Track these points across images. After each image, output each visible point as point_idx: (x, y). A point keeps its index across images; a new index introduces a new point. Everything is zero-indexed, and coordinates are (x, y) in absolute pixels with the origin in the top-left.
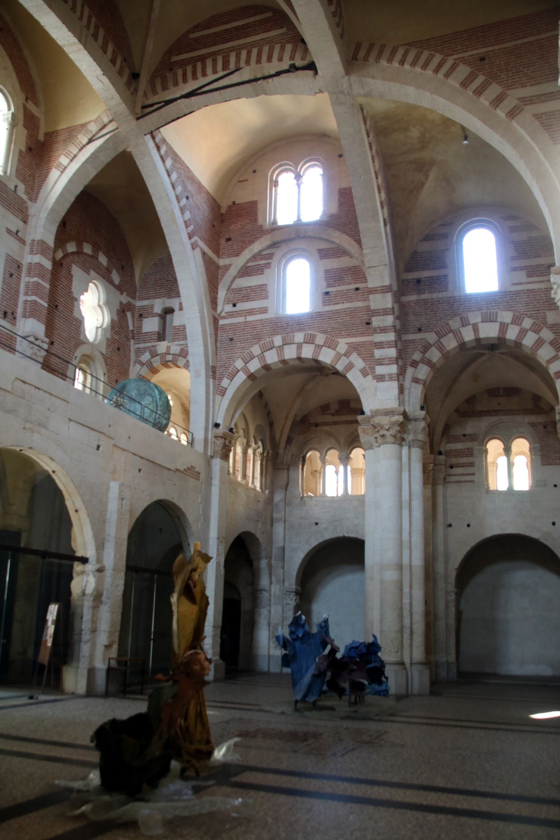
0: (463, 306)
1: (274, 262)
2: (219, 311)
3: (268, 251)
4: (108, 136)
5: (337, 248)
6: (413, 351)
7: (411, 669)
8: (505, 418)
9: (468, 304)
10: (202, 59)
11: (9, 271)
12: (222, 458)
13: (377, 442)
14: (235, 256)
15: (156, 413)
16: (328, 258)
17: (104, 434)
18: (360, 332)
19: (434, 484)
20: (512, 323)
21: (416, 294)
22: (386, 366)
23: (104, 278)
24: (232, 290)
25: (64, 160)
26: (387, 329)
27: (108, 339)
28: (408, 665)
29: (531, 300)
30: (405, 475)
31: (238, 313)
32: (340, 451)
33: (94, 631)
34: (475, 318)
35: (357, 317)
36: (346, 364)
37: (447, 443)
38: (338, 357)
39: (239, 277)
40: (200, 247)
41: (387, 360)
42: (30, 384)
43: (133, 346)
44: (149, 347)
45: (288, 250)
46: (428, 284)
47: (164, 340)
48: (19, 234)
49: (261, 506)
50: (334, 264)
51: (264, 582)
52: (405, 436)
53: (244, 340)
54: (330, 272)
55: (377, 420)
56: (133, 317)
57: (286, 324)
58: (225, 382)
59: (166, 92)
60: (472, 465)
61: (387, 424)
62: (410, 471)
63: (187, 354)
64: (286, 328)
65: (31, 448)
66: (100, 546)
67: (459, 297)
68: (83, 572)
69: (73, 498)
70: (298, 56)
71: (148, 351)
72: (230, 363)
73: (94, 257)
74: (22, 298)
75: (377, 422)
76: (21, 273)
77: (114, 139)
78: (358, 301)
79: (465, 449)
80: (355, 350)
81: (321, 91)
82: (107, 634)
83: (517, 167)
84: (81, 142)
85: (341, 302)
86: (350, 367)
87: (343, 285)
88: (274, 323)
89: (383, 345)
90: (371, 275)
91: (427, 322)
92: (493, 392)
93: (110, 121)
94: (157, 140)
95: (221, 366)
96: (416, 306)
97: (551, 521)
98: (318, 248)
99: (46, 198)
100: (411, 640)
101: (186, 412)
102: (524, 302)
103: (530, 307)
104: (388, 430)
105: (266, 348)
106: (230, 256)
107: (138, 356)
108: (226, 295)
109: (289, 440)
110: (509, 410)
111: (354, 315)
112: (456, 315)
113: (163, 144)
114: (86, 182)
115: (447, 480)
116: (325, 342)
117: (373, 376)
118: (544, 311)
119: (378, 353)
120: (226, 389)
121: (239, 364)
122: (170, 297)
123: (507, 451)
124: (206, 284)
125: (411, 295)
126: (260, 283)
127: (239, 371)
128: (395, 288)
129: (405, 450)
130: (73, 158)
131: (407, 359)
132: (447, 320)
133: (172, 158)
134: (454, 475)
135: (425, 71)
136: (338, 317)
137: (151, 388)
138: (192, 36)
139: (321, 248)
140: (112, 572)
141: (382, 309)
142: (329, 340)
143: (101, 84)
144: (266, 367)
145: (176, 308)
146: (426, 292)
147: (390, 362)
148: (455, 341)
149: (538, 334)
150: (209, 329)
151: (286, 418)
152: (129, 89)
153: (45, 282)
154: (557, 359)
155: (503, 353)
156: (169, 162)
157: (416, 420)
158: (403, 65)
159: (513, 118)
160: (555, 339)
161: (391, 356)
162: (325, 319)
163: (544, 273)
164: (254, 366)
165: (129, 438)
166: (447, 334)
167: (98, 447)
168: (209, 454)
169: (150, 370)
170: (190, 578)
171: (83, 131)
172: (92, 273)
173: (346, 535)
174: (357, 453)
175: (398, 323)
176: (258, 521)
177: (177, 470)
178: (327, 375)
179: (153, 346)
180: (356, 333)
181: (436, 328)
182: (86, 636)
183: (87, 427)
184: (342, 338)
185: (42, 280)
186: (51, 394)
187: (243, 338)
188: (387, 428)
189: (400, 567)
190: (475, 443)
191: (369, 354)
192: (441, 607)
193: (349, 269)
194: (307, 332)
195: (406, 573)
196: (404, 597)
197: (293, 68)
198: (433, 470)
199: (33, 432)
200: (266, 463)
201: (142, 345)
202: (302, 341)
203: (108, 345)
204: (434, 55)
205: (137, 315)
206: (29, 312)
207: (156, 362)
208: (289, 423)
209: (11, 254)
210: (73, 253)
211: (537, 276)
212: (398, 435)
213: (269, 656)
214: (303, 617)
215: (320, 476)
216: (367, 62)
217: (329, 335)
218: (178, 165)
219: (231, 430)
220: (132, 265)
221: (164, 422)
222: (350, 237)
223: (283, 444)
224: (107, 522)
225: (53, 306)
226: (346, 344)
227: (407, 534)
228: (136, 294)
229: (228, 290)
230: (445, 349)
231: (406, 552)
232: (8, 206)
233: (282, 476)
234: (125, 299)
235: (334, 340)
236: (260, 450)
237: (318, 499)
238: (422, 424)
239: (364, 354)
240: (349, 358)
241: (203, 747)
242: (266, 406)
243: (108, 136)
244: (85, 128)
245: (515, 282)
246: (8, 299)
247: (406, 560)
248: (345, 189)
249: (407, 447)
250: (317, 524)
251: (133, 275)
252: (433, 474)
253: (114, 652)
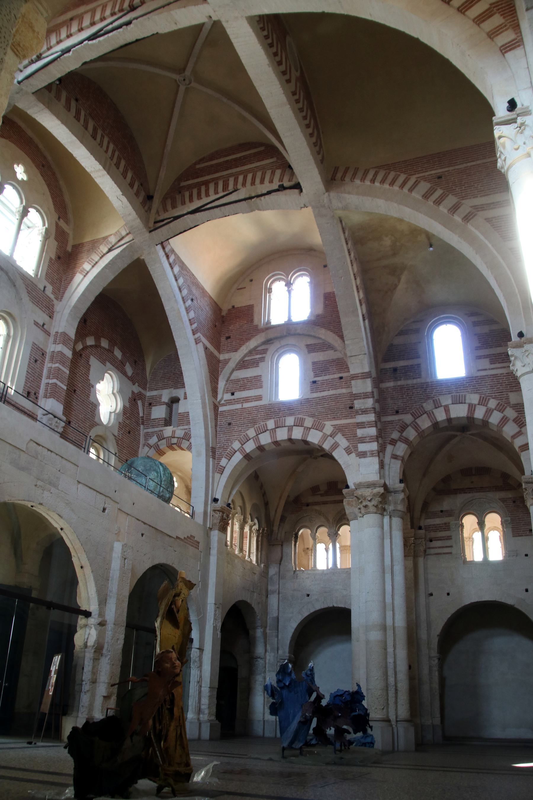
0: (435, 390)
1: (268, 356)
2: (218, 400)
3: (263, 347)
4: (125, 246)
5: (323, 343)
6: (392, 431)
7: (396, 726)
8: (477, 495)
9: (439, 388)
10: (206, 183)
11: (34, 357)
12: (219, 530)
13: (360, 512)
14: (234, 352)
15: (161, 486)
16: (315, 352)
17: (110, 498)
18: (344, 416)
19: (415, 557)
20: (479, 404)
21: (394, 381)
22: (367, 444)
23: (118, 369)
24: (230, 381)
25: (87, 266)
26: (367, 411)
27: (120, 423)
28: (393, 723)
29: (494, 384)
30: (387, 542)
31: (236, 400)
32: (329, 528)
33: (94, 682)
34: (446, 400)
35: (341, 403)
36: (332, 444)
37: (426, 519)
38: (325, 437)
39: (236, 370)
40: (203, 343)
41: (369, 438)
42: (43, 447)
43: (143, 431)
44: (157, 432)
45: (279, 346)
46: (403, 372)
47: (170, 425)
48: (45, 327)
49: (256, 577)
50: (320, 356)
51: (260, 650)
52: (386, 506)
53: (241, 425)
54: (317, 364)
55: (359, 492)
56: (143, 405)
57: (278, 409)
58: (223, 462)
59: (175, 210)
60: (449, 538)
61: (369, 496)
62: (391, 539)
63: (190, 437)
64: (278, 413)
65: (41, 504)
66: (103, 602)
67: (431, 382)
68: (86, 626)
69: (79, 555)
70: (286, 178)
71: (156, 435)
72: (228, 444)
73: (110, 351)
74: (44, 381)
75: (360, 493)
76: (45, 360)
77: (131, 248)
78: (342, 388)
79: (442, 524)
80: (339, 431)
81: (305, 206)
82: (106, 685)
83: (474, 262)
84: (102, 252)
85: (327, 389)
86: (336, 446)
87: (329, 375)
88: (267, 409)
89: (364, 425)
90: (352, 363)
91: (403, 405)
92: (466, 472)
93: (127, 234)
94: (167, 250)
95: (220, 447)
96: (393, 391)
97: (524, 588)
98: (306, 344)
99: (70, 297)
100: (396, 697)
101: (189, 491)
102: (489, 386)
103: (494, 390)
104: (370, 501)
105: (260, 431)
106: (229, 351)
107: (146, 439)
108: (226, 385)
109: (283, 519)
110: (481, 488)
111: (338, 401)
112: (428, 398)
113: (172, 254)
114: (104, 283)
115: (427, 553)
116: (313, 425)
117: (356, 454)
118: (507, 393)
119: (360, 432)
120: (225, 468)
121: (236, 445)
122: (176, 388)
123: (481, 525)
124: (208, 374)
125: (388, 382)
126: (255, 374)
127: (236, 452)
128: (374, 375)
129: (386, 519)
130: (95, 264)
131: (386, 438)
132: (421, 403)
133: (179, 266)
134: (433, 548)
135: (392, 187)
136: (324, 403)
137: (156, 465)
138: (198, 166)
139: (309, 343)
140: (113, 626)
141: (363, 393)
142: (316, 423)
143: (121, 202)
144: (261, 448)
145: (182, 397)
146: (402, 379)
147: (371, 440)
148: (429, 421)
149: (502, 413)
150: (210, 414)
151: (280, 498)
152: (144, 207)
153: (65, 368)
154: (521, 434)
155: (472, 435)
156: (176, 269)
157: (396, 492)
158: (374, 183)
159: (468, 222)
160: (518, 416)
161: (372, 435)
162: (313, 405)
163: (505, 360)
164: (250, 447)
165: (133, 504)
166: (422, 415)
167: (104, 510)
168: (208, 526)
169: (157, 452)
170: (173, 602)
171: (104, 242)
172: (108, 364)
173: (335, 605)
174: (344, 530)
175: (377, 406)
176: (254, 592)
177: (178, 538)
178: (316, 458)
179: (160, 431)
180: (341, 416)
181: (412, 410)
182: (86, 687)
183: (94, 490)
184: (328, 421)
185: (63, 366)
186: (62, 457)
187: (239, 423)
188: (369, 499)
189: (384, 628)
190: (451, 518)
191: (352, 434)
192: (425, 671)
193: (334, 361)
194: (297, 416)
195: (390, 633)
196: (388, 656)
197: (282, 188)
198: (414, 543)
199: (43, 490)
200: (262, 539)
201: (150, 430)
202: (293, 424)
203: (120, 428)
204: (399, 175)
205: (146, 404)
206: (49, 393)
207: (163, 445)
208: (283, 503)
209: (36, 343)
210: (91, 346)
211: (499, 363)
212: (380, 506)
213: (264, 721)
214: (290, 666)
215: (312, 553)
216: (344, 182)
217: (316, 418)
218: (185, 272)
219: (229, 505)
220: (144, 361)
221: (168, 496)
222: (334, 333)
223: (277, 523)
224: (110, 579)
225: (72, 390)
226: (332, 426)
227: (390, 597)
228: (146, 385)
229: (227, 381)
230: (420, 428)
231: (389, 614)
232: (36, 303)
233: (276, 553)
234: (136, 389)
235: (321, 423)
236: (256, 527)
237: (309, 572)
238: (402, 496)
239: (348, 435)
240: (334, 439)
241: (182, 769)
242: (261, 487)
243: (125, 246)
244: (106, 240)
245: (480, 368)
246: (31, 380)
247: (389, 622)
248: (330, 293)
249: (388, 517)
250: (308, 595)
251: (144, 369)
252: (414, 547)
253: (112, 703)
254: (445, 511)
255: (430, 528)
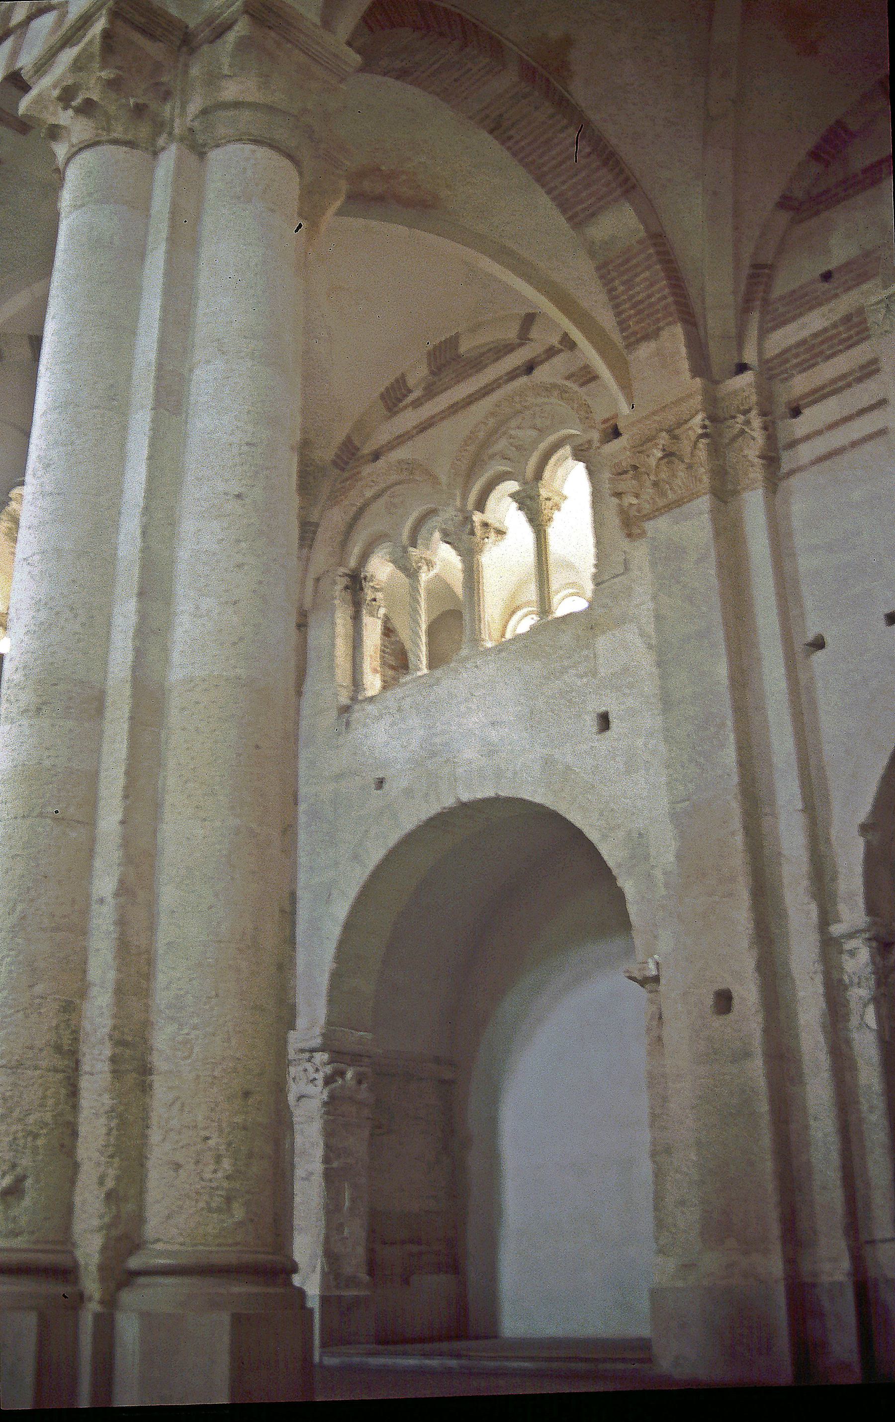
79: (835, 326)
115: (785, 467)
134: (808, 438)
254: (840, 269)
255: (787, 361)
